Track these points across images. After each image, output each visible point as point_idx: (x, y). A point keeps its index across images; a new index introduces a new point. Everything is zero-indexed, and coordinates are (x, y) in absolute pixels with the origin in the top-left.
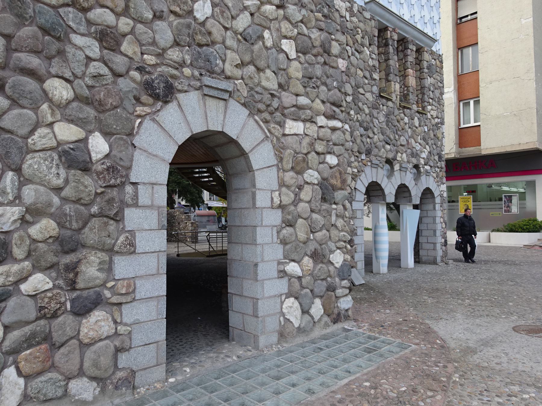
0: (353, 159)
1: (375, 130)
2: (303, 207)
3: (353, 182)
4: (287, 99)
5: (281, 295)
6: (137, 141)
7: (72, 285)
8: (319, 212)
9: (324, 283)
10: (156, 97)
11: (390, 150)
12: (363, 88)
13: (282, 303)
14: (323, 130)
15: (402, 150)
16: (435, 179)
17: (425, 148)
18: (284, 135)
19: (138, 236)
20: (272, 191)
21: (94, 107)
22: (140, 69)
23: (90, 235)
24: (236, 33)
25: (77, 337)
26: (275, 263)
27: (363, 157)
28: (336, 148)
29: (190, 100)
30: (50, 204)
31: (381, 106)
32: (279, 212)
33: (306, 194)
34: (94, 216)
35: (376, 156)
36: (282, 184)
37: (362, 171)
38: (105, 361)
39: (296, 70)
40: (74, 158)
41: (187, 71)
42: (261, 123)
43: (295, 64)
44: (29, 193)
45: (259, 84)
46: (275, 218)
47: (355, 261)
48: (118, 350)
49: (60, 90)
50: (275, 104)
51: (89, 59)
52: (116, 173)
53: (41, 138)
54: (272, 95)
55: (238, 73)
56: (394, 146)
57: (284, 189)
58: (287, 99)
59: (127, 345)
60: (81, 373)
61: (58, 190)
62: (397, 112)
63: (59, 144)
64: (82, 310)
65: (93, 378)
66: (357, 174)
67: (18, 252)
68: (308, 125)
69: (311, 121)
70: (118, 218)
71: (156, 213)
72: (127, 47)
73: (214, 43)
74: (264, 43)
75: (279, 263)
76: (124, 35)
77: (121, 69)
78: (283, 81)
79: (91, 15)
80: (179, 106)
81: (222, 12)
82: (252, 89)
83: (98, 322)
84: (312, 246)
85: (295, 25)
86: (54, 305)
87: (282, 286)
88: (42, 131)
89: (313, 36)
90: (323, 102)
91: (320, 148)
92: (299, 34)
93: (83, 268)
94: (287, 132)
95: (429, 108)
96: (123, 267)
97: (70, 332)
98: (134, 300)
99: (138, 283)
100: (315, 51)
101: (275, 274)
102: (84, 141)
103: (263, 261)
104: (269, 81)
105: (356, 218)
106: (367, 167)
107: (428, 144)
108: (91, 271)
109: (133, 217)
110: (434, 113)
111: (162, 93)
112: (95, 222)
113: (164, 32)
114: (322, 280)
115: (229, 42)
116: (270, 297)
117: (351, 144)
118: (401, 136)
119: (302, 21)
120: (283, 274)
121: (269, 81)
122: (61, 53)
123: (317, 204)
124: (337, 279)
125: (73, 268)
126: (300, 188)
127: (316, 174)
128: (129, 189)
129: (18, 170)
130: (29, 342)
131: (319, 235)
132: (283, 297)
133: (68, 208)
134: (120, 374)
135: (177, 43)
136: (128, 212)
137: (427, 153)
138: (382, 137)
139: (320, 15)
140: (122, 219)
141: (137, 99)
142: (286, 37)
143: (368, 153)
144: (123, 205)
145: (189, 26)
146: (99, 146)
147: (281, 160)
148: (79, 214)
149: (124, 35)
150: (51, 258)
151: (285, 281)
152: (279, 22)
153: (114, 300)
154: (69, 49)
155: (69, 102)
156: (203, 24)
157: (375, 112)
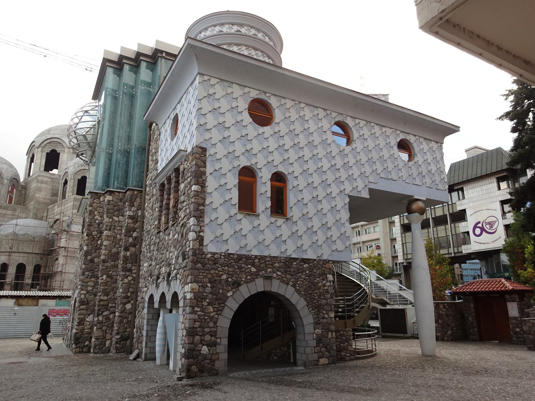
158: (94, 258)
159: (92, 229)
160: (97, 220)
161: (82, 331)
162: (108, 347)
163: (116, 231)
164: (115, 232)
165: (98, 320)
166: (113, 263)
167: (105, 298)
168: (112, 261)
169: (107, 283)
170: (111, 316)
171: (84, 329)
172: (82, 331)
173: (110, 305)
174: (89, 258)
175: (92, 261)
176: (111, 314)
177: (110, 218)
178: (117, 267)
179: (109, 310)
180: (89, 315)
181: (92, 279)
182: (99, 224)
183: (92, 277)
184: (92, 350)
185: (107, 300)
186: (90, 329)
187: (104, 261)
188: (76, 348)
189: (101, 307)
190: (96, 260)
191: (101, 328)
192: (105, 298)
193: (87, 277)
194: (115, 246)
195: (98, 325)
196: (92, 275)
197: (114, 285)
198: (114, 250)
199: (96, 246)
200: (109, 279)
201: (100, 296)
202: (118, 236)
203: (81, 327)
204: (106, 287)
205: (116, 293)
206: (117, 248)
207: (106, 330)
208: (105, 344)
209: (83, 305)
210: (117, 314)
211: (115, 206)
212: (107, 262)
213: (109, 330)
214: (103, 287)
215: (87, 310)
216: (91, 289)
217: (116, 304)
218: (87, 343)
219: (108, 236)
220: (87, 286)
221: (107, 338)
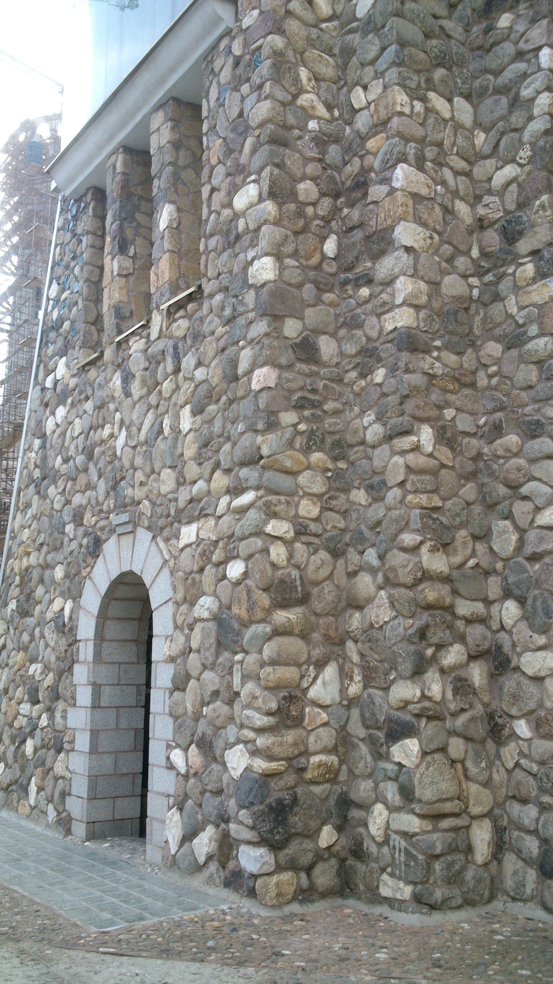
158: (317, 332)
159: (292, 161)
160: (307, 114)
161: (296, 762)
162: (486, 865)
163: (448, 174)
164: (443, 183)
165: (424, 697)
166: (451, 358)
167: (437, 563)
168: (446, 347)
169: (435, 473)
170: (477, 674)
171: (306, 753)
172: (296, 762)
173: (464, 608)
174: (292, 328)
175: (306, 349)
176: (472, 658)
177: (417, 95)
178: (473, 385)
179: (462, 639)
180: (320, 665)
181: (317, 457)
182: (322, 141)
183: (313, 441)
184: (390, 886)
185: (447, 579)
186: (333, 750)
187: (411, 342)
188: (279, 868)
189: (425, 618)
190: (327, 347)
191: (443, 750)
192: (437, 563)
193: (290, 444)
194: (450, 260)
195: (428, 729)
196: (311, 434)
197: (469, 491)
198: (452, 285)
199: (318, 267)
200: (445, 454)
201: (415, 549)
202: (462, 207)
203: (290, 736)
204: (437, 502)
205: (482, 536)
206: (465, 277)
207: (463, 762)
208: (469, 849)
209: (285, 605)
211: (427, 36)
212: (427, 352)
213: (478, 756)
214: (423, 499)
215: (304, 636)
216: (315, 512)
217: (488, 603)
218: (327, 836)
219: (416, 197)
220: (293, 495)
221: (476, 810)
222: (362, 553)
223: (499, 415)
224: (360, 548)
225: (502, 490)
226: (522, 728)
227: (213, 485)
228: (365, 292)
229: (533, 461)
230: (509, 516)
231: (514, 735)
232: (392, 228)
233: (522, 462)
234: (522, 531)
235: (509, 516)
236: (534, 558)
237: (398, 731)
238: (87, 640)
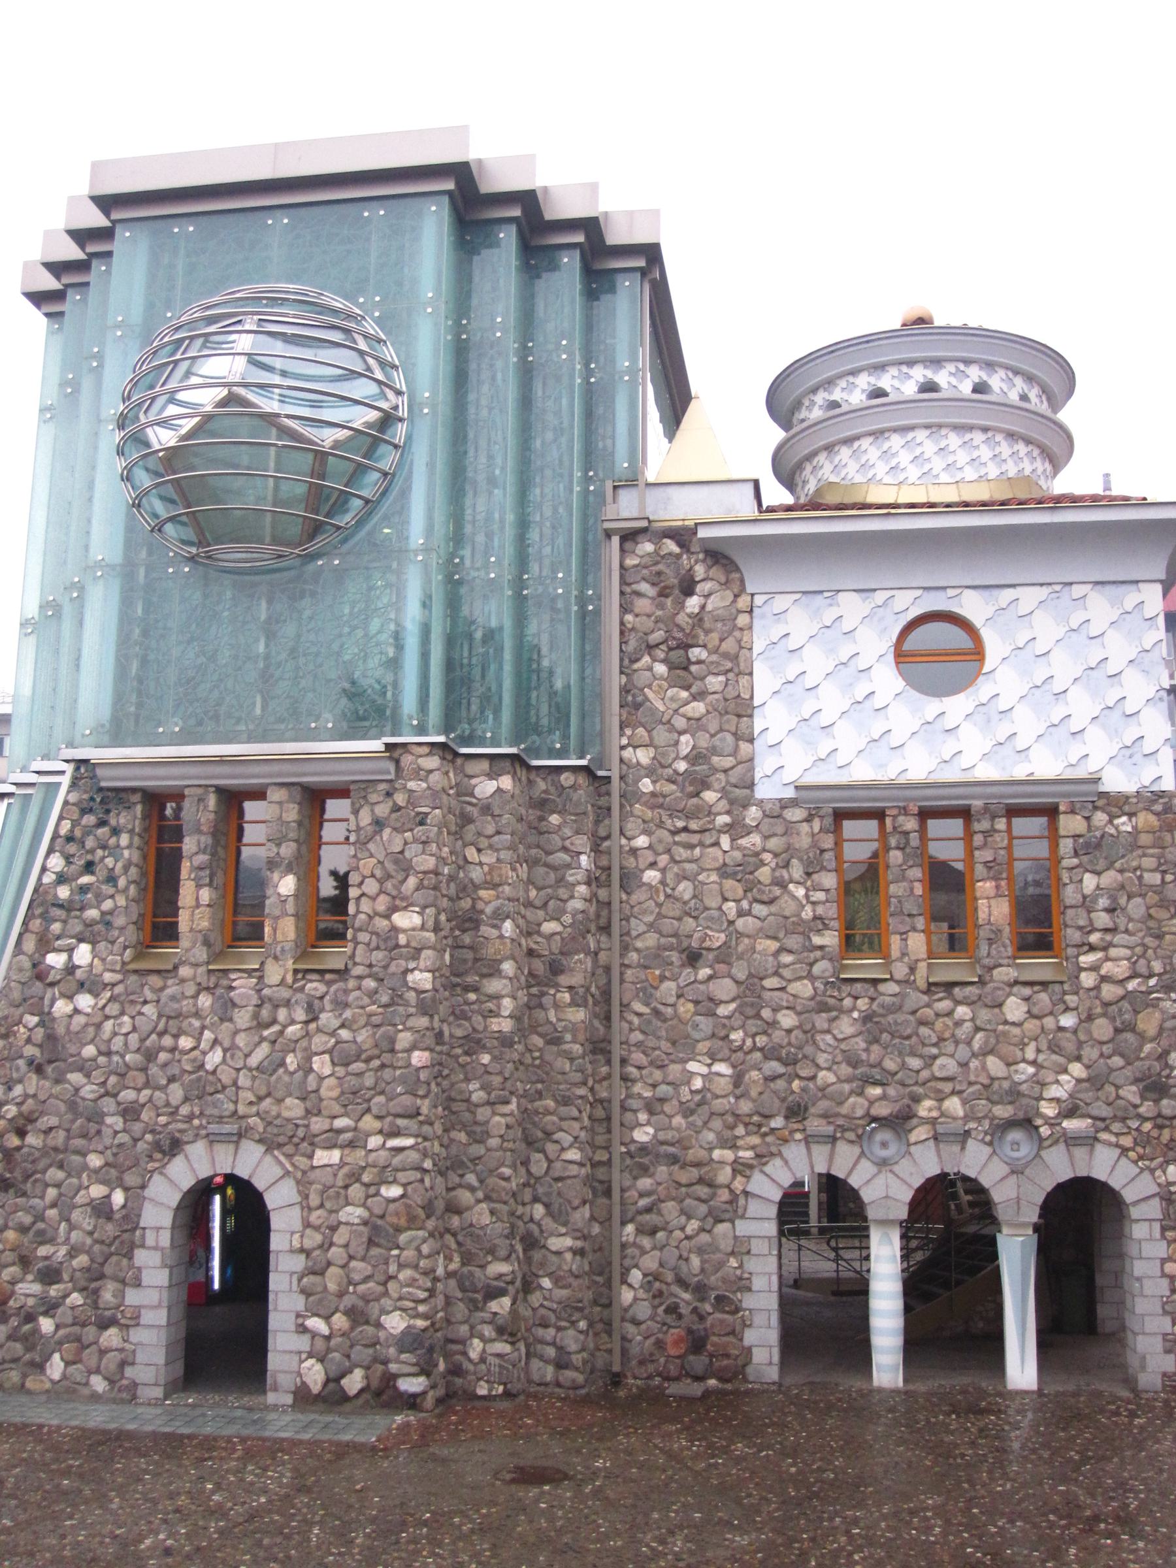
0: (740, 1130)
1: (822, 1059)
2: (335, 1253)
3: (739, 1178)
4: (318, 1124)
5: (300, 1353)
6: (147, 1193)
7: (95, 1302)
8: (363, 1259)
9: (371, 1351)
10: (164, 1153)
11: (884, 1097)
12: (776, 973)
13: (302, 1362)
14: (374, 1154)
15: (940, 1091)
16: (1125, 1151)
17: (1065, 1071)
18: (313, 1168)
19: (144, 1273)
20: (292, 1233)
21: (116, 1171)
22: (152, 1132)
23: (108, 1269)
24: (250, 1070)
25: (96, 1343)
26: (293, 1316)
27: (777, 1122)
28: (400, 1175)
29: (197, 1150)
30: (84, 1244)
31: (848, 1002)
32: (303, 1257)
33: (341, 1237)
34: (112, 1254)
35: (825, 1116)
36: (307, 1225)
37: (772, 1154)
38: (113, 1367)
39: (329, 1090)
40: (102, 1209)
41: (196, 1122)
42: (282, 1158)
43: (326, 1082)
44: (75, 1236)
45: (278, 1116)
46: (298, 1263)
47: (747, 1342)
48: (123, 1364)
49: (95, 1161)
50: (301, 1132)
51: (116, 1133)
52: (130, 1219)
53: (80, 1199)
54: (297, 1126)
55: (254, 1109)
56: (904, 1085)
57: (308, 1231)
58: (318, 1124)
59: (130, 1360)
60: (98, 1371)
61: (91, 1233)
62: (916, 999)
63: (92, 1200)
64: (104, 1325)
65: (106, 1378)
66: (754, 1162)
67: (66, 1277)
68: (347, 1151)
69: (351, 1145)
70: (129, 1256)
71: (159, 1254)
72: (144, 1116)
73: (224, 1088)
74: (286, 1071)
75: (298, 1316)
76: (143, 1105)
77: (137, 1135)
78: (309, 1104)
79: (120, 1098)
80: (186, 1157)
81: (232, 1056)
82: (270, 1123)
83: (111, 1337)
84: (347, 1301)
85: (333, 1034)
86: (83, 1317)
87: (303, 1343)
88: (82, 1192)
89: (359, 1039)
90: (379, 1117)
91: (366, 1178)
92: (337, 1043)
93: (102, 1293)
94: (315, 1163)
95: (1086, 959)
96: (132, 1297)
97: (91, 1339)
98: (138, 1325)
99: (143, 1311)
100: (363, 1056)
101: (293, 1328)
102: (108, 1196)
103: (275, 1309)
104: (293, 1108)
105: (748, 1252)
106: (793, 1145)
107: (1078, 1058)
108: (108, 1296)
109: (142, 1257)
110: (1119, 969)
111: (173, 1147)
112: (114, 1259)
113: (176, 1092)
114: (366, 1346)
115: (240, 1083)
116: (285, 1352)
117: (732, 1100)
118: (935, 1057)
119: (343, 1026)
120: (302, 1329)
121: (293, 1108)
122: (99, 1132)
123: (358, 1248)
124: (392, 1350)
125: (96, 1292)
126: (334, 1229)
127: (360, 1211)
128: (138, 1233)
129: (68, 1220)
130: (67, 1339)
131: (361, 1288)
132: (304, 1356)
133: (97, 1248)
134: (125, 1382)
135: (186, 1099)
136: (136, 1251)
137: (1069, 1086)
138: (845, 1070)
139: (374, 1007)
140: (131, 1258)
141: (150, 1157)
142: (317, 1054)
143: (796, 1112)
144: (132, 1246)
145: (199, 1079)
146: (118, 1198)
147: (307, 1197)
148: (102, 1252)
149: (143, 1105)
150: (83, 1283)
151: (306, 1338)
152: (311, 1038)
153: (123, 1321)
154: (104, 1129)
155: (101, 1168)
156: (214, 1072)
157: (821, 1021)
210: (560, 1243)
222: (462, 1176)
223: (539, 1086)
224: (460, 1172)
225: (540, 1134)
226: (546, 1283)
227: (361, 1124)
228: (472, 996)
229: (561, 1119)
230: (543, 1151)
231: (541, 1288)
232: (500, 962)
233: (555, 1118)
234: (550, 1161)
235: (543, 1151)
236: (557, 1179)
237: (493, 1293)
238: (158, 1229)
